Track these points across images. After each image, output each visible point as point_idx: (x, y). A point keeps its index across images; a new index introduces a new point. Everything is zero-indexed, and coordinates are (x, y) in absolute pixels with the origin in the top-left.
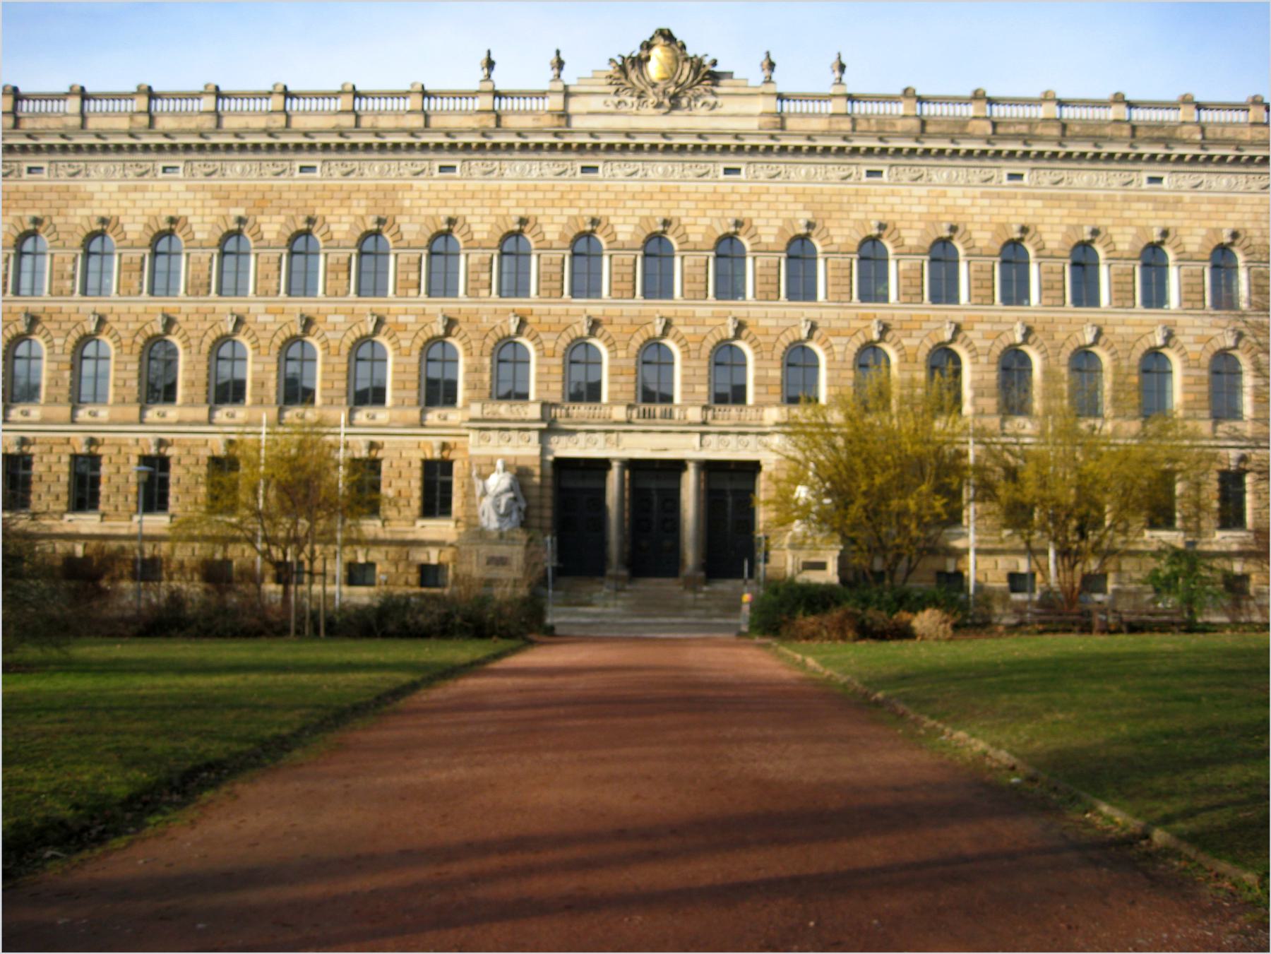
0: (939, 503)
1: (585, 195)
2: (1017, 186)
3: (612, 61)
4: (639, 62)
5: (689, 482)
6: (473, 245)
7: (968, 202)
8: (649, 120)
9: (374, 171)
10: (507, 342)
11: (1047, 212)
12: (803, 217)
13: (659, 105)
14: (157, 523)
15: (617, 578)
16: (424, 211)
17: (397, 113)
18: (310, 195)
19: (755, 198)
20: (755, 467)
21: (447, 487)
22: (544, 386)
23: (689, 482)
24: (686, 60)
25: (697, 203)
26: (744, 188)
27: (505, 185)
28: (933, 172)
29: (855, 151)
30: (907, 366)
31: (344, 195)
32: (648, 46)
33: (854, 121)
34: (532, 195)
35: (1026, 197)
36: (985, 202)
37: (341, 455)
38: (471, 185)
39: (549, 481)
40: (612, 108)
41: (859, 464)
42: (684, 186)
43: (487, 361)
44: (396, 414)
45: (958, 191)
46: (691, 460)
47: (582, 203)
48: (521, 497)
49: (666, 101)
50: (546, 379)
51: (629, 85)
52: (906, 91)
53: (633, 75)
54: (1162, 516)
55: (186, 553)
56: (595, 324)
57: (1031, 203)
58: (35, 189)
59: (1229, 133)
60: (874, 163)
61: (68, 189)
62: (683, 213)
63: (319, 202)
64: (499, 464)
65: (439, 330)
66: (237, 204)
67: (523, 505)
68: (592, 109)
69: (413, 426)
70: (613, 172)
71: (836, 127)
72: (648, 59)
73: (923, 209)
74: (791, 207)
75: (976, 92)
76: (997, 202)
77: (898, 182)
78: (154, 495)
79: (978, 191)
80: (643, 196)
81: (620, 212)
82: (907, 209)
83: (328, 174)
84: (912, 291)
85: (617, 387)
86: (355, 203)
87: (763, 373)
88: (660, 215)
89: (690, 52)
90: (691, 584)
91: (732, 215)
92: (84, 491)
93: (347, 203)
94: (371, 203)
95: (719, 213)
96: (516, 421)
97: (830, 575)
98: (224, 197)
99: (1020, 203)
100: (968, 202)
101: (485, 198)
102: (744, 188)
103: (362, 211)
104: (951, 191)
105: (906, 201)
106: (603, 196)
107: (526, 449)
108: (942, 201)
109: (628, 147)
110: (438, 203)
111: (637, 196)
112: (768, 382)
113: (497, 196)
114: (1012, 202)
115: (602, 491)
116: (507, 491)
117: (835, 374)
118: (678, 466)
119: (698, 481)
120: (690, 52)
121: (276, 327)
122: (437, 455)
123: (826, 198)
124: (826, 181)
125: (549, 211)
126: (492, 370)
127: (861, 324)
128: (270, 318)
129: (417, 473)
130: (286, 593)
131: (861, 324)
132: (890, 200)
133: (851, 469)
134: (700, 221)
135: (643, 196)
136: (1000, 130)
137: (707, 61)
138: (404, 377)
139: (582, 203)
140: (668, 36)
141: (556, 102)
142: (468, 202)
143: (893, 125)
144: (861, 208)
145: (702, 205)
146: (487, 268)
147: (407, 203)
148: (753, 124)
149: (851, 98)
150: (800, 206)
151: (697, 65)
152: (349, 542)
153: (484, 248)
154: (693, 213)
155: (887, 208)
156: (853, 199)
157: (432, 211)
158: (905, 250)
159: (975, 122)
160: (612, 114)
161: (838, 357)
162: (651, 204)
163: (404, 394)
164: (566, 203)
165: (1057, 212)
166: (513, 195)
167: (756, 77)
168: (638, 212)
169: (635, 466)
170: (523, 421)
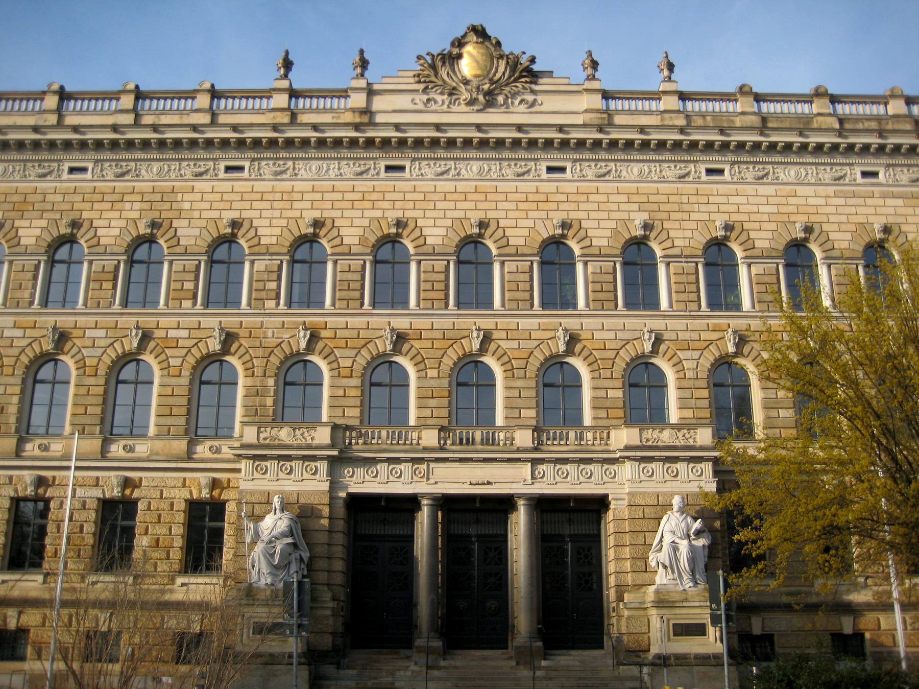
2: (873, 185)
3: (419, 58)
4: (451, 59)
5: (519, 524)
6: (260, 250)
7: (822, 201)
8: (461, 116)
9: (151, 173)
10: (296, 360)
11: (910, 211)
12: (639, 218)
13: (471, 102)
15: (428, 651)
16: (205, 214)
18: (79, 198)
19: (584, 198)
20: (600, 504)
21: (218, 534)
23: (519, 524)
24: (501, 57)
25: (519, 204)
26: (571, 187)
27: (299, 186)
28: (779, 170)
29: (694, 145)
31: (117, 197)
33: (688, 117)
34: (327, 196)
35: (884, 196)
36: (841, 201)
38: (260, 186)
39: (341, 525)
40: (421, 106)
42: (503, 186)
43: (271, 382)
44: (159, 445)
45: (809, 190)
46: (520, 496)
47: (386, 205)
48: (302, 544)
49: (481, 97)
50: (343, 402)
51: (440, 83)
52: (741, 88)
53: (443, 72)
56: (400, 338)
57: (889, 202)
60: (714, 160)
63: (88, 206)
64: (276, 502)
65: (214, 345)
67: (306, 555)
68: (398, 107)
69: (178, 459)
70: (422, 173)
72: (460, 56)
74: (623, 207)
75: (817, 89)
76: (852, 201)
77: (742, 181)
79: (830, 190)
80: (456, 196)
81: (428, 214)
82: (755, 209)
83: (100, 175)
84: (769, 298)
85: (428, 412)
86: (128, 206)
87: (602, 393)
88: (475, 216)
89: (506, 49)
90: (526, 657)
91: (558, 217)
93: (118, 206)
94: (146, 206)
95: (543, 215)
99: (880, 202)
100: (822, 201)
102: (571, 187)
103: (136, 215)
104: (801, 190)
105: (751, 200)
107: (312, 484)
108: (792, 200)
109: (438, 144)
111: (449, 197)
112: (608, 404)
113: (288, 198)
114: (869, 201)
115: (410, 538)
116: (284, 535)
117: (687, 393)
118: (506, 503)
119: (531, 523)
120: (506, 49)
121: (24, 343)
122: (205, 494)
123: (664, 199)
124: (663, 180)
125: (347, 213)
126: (276, 392)
127: (714, 336)
128: (19, 333)
129: (180, 518)
131: (714, 336)
132: (733, 199)
134: (521, 223)
135: (456, 196)
136: (847, 126)
137: (524, 60)
138: (171, 401)
139: (386, 205)
140: (481, 33)
141: (358, 100)
142: (256, 205)
144: (703, 208)
145: (522, 206)
146: (275, 276)
147: (187, 206)
149: (683, 96)
150: (635, 207)
151: (513, 63)
153: (272, 254)
154: (511, 214)
155: (733, 208)
156: (693, 199)
157: (215, 214)
158: (756, 252)
159: (820, 118)
163: (169, 421)
164: (368, 205)
167: (579, 75)
168: (450, 214)
169: (448, 504)
170: (309, 447)
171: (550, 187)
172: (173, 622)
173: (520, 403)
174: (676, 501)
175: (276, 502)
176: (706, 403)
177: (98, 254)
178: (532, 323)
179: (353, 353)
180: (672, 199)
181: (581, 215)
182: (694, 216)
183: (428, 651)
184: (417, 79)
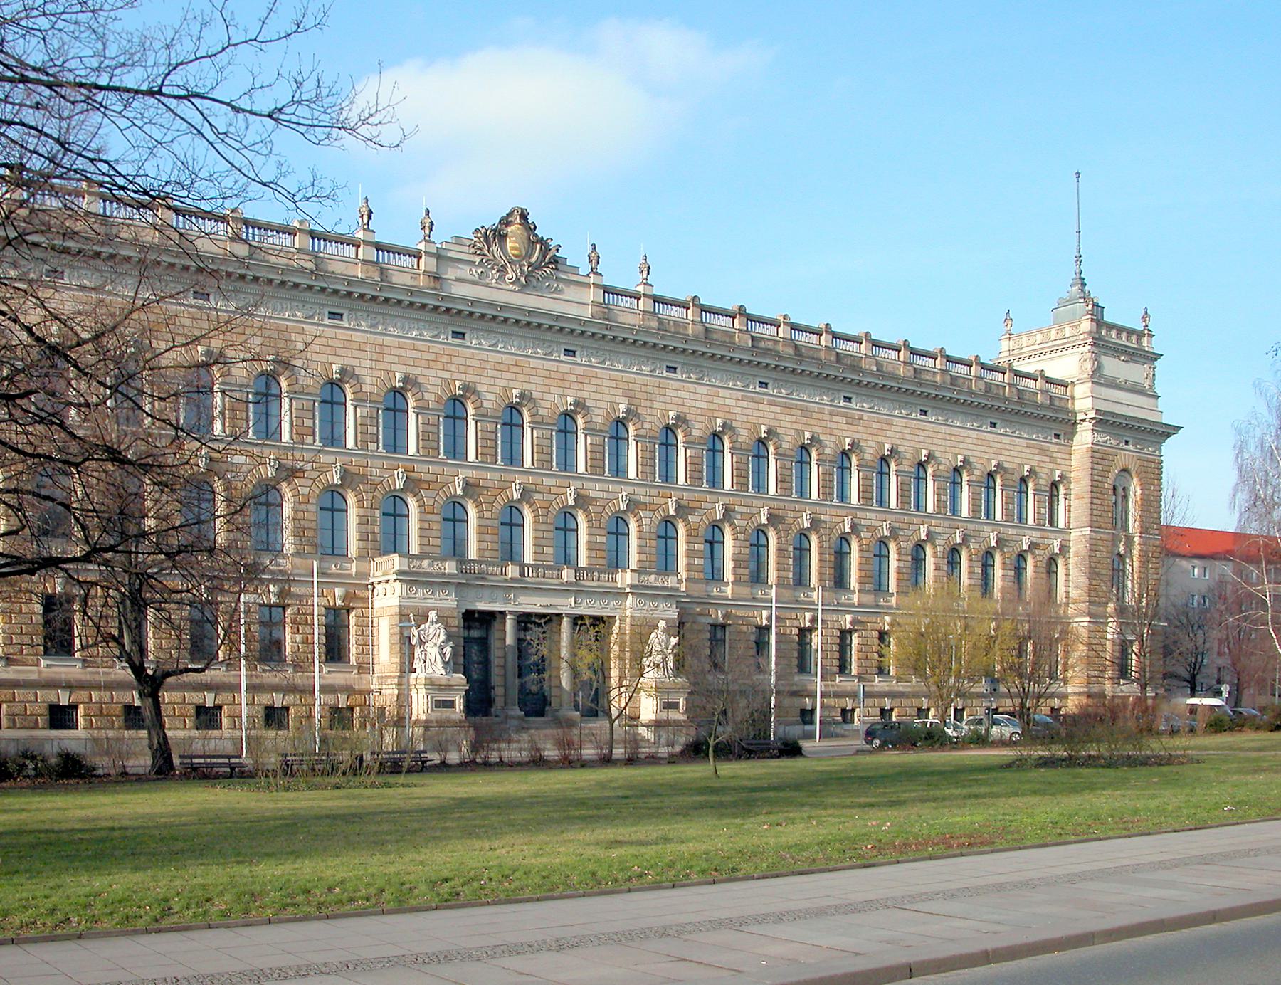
1: (455, 360)
8: (506, 294)
22: (425, 541)
26: (579, 370)
27: (388, 340)
30: (692, 539)
32: (506, 221)
34: (410, 353)
36: (744, 404)
38: (358, 336)
42: (534, 363)
49: (523, 279)
53: (494, 248)
57: (773, 408)
62: (533, 387)
71: (647, 323)
73: (704, 405)
85: (485, 545)
95: (560, 391)
96: (437, 575)
99: (767, 408)
100: (733, 403)
101: (376, 353)
106: (470, 362)
108: (716, 400)
109: (495, 320)
110: (328, 350)
123: (637, 387)
125: (426, 372)
127: (662, 501)
131: (662, 501)
139: (453, 368)
143: (686, 328)
144: (662, 398)
145: (548, 382)
158: (692, 439)
160: (476, 283)
161: (646, 529)
162: (509, 376)
164: (440, 365)
165: (788, 418)
166: (394, 351)
167: (585, 268)
171: (565, 368)
173: (544, 542)
174: (662, 624)
175: (433, 615)
176: (654, 550)
177: (230, 384)
178: (551, 482)
179: (433, 493)
180: (644, 388)
181: (585, 395)
182: (656, 405)
184: (472, 250)
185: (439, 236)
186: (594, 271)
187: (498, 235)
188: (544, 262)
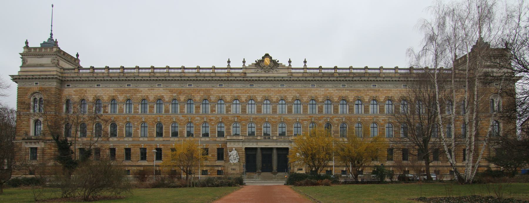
0: (327, 156)
9: (205, 86)
14: (159, 163)
15: (259, 172)
17: (209, 73)
26: (285, 89)
27: (233, 89)
37: (199, 147)
38: (226, 89)
41: (309, 148)
44: (211, 139)
45: (331, 89)
54: (375, 158)
55: (167, 169)
58: (129, 90)
59: (390, 75)
61: (136, 90)
64: (234, 149)
66: (175, 93)
70: (257, 87)
78: (159, 157)
89: (273, 59)
92: (144, 156)
97: (303, 172)
98: (171, 91)
102: (285, 89)
104: (329, 89)
109: (259, 80)
120: (273, 59)
129: (216, 151)
130: (187, 177)
133: (308, 149)
148: (286, 75)
152: (201, 166)
167: (287, 65)
172: (217, 168)
175: (234, 149)
183: (259, 172)
185: (247, 65)
186: (290, 65)
187: (262, 61)
188: (275, 64)
